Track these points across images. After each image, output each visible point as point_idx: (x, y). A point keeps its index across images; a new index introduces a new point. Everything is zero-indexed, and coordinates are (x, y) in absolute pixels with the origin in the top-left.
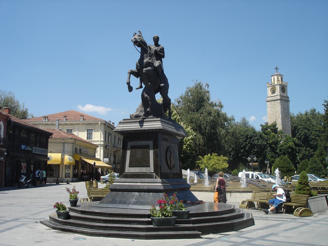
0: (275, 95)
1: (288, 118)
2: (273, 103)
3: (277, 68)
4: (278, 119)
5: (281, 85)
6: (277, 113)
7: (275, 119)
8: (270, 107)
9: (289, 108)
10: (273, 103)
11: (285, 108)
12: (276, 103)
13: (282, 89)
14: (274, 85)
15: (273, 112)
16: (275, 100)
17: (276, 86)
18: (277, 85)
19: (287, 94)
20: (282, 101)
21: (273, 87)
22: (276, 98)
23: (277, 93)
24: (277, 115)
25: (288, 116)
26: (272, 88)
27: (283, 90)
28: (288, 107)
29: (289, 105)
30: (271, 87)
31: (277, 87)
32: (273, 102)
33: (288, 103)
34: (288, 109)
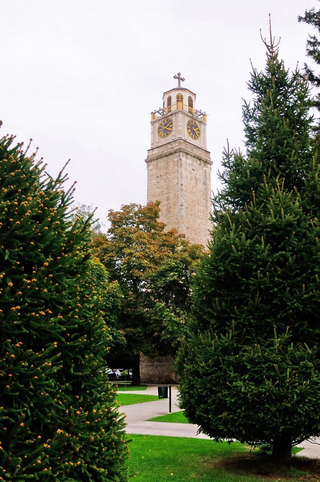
0: (169, 139)
2: (162, 164)
3: (182, 77)
4: (173, 207)
5: (187, 115)
6: (171, 191)
8: (155, 176)
9: (208, 182)
10: (162, 164)
11: (196, 179)
12: (171, 164)
13: (188, 125)
14: (168, 116)
15: (162, 190)
16: (166, 156)
17: (173, 118)
18: (175, 113)
19: (205, 143)
20: (187, 158)
21: (164, 122)
22: (172, 148)
23: (175, 136)
24: (172, 196)
25: (204, 201)
26: (161, 125)
27: (191, 129)
28: (206, 178)
29: (210, 175)
30: (161, 121)
31: (174, 120)
32: (162, 160)
33: (207, 167)
34: (205, 183)
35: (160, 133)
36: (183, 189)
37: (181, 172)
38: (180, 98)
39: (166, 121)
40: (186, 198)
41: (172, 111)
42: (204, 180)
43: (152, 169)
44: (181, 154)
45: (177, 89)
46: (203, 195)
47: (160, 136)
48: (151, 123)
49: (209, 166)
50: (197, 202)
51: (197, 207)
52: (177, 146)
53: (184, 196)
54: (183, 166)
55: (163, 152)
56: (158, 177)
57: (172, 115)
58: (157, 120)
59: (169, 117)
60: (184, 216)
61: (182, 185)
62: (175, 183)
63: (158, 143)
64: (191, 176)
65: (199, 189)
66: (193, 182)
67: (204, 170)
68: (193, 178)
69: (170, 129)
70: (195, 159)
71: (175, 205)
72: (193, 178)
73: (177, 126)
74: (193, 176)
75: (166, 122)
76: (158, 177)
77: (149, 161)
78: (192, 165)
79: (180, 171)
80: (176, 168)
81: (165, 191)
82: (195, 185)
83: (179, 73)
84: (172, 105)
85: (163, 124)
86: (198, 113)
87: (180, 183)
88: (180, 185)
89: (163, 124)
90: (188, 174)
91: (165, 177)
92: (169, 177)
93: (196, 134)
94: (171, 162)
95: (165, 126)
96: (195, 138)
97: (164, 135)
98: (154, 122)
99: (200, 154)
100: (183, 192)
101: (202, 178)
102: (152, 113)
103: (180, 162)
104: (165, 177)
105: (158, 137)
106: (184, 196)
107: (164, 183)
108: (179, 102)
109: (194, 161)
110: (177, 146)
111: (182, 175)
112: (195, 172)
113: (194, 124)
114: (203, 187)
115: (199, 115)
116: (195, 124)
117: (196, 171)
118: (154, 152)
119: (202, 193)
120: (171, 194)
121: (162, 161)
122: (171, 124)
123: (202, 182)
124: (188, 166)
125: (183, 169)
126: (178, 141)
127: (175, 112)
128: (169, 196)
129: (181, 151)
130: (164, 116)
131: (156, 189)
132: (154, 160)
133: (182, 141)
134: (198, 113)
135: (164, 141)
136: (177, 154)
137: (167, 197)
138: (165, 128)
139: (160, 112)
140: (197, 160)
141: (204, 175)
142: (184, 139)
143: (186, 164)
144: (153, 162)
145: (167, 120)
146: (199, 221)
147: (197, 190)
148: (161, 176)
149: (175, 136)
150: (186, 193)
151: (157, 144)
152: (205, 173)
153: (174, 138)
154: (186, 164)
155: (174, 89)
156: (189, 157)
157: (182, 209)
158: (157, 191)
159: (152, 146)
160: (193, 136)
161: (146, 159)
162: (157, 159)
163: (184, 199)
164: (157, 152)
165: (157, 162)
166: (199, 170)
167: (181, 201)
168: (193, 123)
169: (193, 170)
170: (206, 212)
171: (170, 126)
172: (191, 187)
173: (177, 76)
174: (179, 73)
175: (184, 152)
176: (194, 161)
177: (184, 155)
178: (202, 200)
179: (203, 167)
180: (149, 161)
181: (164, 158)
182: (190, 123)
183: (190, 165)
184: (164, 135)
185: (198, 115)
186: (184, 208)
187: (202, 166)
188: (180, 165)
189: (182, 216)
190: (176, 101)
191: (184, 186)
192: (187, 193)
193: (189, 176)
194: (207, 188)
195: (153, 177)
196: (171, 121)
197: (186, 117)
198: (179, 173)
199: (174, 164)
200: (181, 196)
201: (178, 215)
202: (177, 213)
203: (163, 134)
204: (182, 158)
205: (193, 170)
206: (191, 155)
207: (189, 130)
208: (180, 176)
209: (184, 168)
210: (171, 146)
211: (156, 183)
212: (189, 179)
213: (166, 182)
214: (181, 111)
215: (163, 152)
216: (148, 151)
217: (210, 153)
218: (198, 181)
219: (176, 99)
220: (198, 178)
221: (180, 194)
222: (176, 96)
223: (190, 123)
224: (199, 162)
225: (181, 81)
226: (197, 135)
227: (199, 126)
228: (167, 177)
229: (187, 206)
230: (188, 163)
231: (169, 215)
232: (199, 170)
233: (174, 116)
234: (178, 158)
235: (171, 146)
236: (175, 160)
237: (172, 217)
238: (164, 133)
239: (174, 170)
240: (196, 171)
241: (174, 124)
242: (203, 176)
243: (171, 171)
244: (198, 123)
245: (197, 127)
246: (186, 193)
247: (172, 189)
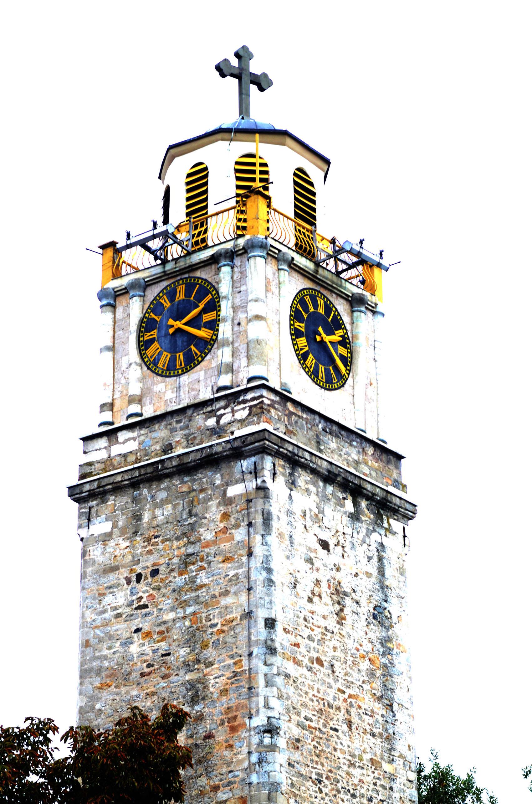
1: (392, 749)
3: (255, 67)
4: (221, 736)
6: (210, 653)
8: (125, 573)
13: (296, 315)
20: (292, 484)
21: (172, 295)
22: (217, 431)
23: (230, 369)
25: (380, 710)
27: (311, 335)
28: (383, 587)
30: (153, 292)
31: (225, 288)
33: (389, 530)
35: (150, 352)
36: (277, 645)
37: (267, 559)
38: (258, 176)
39: (181, 289)
40: (291, 690)
41: (210, 243)
42: (378, 597)
43: (106, 538)
44: (268, 462)
45: (238, 131)
46: (371, 674)
48: (102, 295)
49: (396, 525)
50: (342, 715)
51: (345, 740)
52: (243, 422)
53: (279, 680)
54: (275, 524)
55: (168, 448)
56: (139, 577)
57: (214, 260)
58: (134, 285)
59: (198, 274)
60: (284, 788)
61: (270, 623)
62: (236, 614)
63: (139, 400)
64: (315, 575)
65: (351, 645)
67: (374, 546)
68: (324, 585)
69: (203, 333)
70: (330, 489)
71: (233, 729)
72: (324, 585)
73: (242, 316)
74: (324, 575)
75: (181, 295)
76: (139, 577)
77: (92, 495)
78: (317, 519)
79: (259, 550)
80: (240, 534)
81: (183, 652)
82: (332, 623)
83: (244, 48)
84: (211, 210)
85: (167, 304)
86: (343, 256)
87: (261, 614)
88: (261, 623)
89: (167, 304)
91: (179, 581)
92: (203, 578)
93: (333, 361)
94: (213, 504)
95: (178, 318)
96: (329, 380)
97: (173, 360)
98: (124, 292)
99: (357, 463)
100: (277, 660)
102: (103, 247)
103: (259, 504)
104: (179, 581)
106: (279, 680)
107: (173, 609)
108: (253, 197)
109: (325, 498)
110: (243, 422)
111: (269, 571)
113: (321, 311)
114: (371, 635)
115: (350, 267)
116: (329, 308)
117: (339, 549)
118: (116, 450)
119: (365, 665)
120: (214, 670)
121: (162, 495)
122: (214, 306)
123: (366, 608)
124: (299, 525)
125: (272, 539)
126: (249, 396)
127: (229, 246)
128: (203, 681)
129: (263, 451)
130: (169, 267)
131: (128, 642)
132: (117, 489)
133: (268, 397)
134: (343, 256)
135: (170, 395)
136: (246, 464)
137: (191, 686)
138: (179, 324)
139: (155, 244)
140: (340, 495)
141: (375, 572)
142: (278, 388)
143: (289, 513)
144: (111, 500)
145: (189, 289)
147: (345, 651)
148: (155, 573)
149: (230, 369)
150: (290, 668)
151: (135, 408)
152: (380, 559)
153: (225, 380)
154: (289, 513)
155: (220, 131)
156: (303, 478)
157: (273, 748)
158: (134, 649)
159: (107, 416)
160: (322, 368)
161: (75, 481)
162: (135, 484)
163: (280, 697)
164: (132, 446)
165: (135, 500)
166: (353, 547)
167: (267, 706)
168: (321, 302)
169: (325, 545)
170: (387, 767)
171: (207, 317)
172: (317, 634)
173: (235, 62)
174: (244, 48)
175: (277, 454)
176: (325, 498)
177: (279, 470)
178: (368, 703)
179: (368, 534)
180: (92, 495)
181: (176, 482)
182: (302, 302)
183: (309, 523)
184: (173, 360)
185: (342, 267)
186: (281, 742)
187: (363, 528)
188: (259, 520)
189: (274, 787)
190: (233, 191)
191: (279, 627)
192: (297, 662)
194: (388, 640)
195: (112, 578)
196: (207, 293)
197: (285, 276)
198: (256, 563)
199: (226, 516)
200: (269, 683)
201: (254, 778)
202: (249, 770)
203: (166, 357)
204: (269, 484)
205: (325, 545)
206: (314, 471)
207: (302, 342)
208: (258, 577)
209: (281, 535)
210: (211, 422)
211: (128, 610)
213: (184, 604)
214: (263, 246)
215: (168, 448)
216: (86, 439)
217: (399, 457)
218: (348, 601)
219: (233, 182)
220: (346, 587)
221: (263, 669)
222: (232, 167)
223: (302, 302)
224: (349, 506)
225: (253, 88)
226: (336, 369)
227: (346, 319)
228: (193, 580)
229: (296, 732)
230: (299, 513)
231: (203, 781)
232: (353, 547)
233: (225, 271)
234: (252, 485)
235: (211, 422)
236: (234, 491)
237: (216, 789)
238: (173, 350)
239: (225, 546)
240: (339, 549)
241: (225, 308)
242: (369, 575)
243: (212, 550)
244: (341, 307)
245: (338, 324)
246: (290, 668)
247: (216, 644)
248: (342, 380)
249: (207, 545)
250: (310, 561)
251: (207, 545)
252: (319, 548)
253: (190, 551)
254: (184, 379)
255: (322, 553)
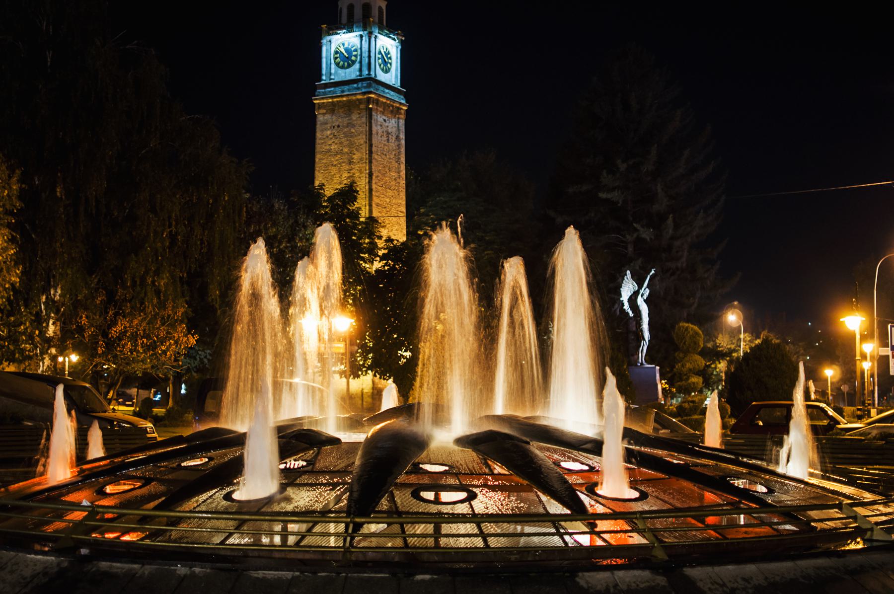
7: (346, 175)
8: (328, 126)
11: (388, 133)
25: (397, 165)
47: (337, 64)
66: (385, 138)
74: (385, 129)
90: (379, 127)
97: (344, 64)
101: (394, 130)
105: (333, 66)
112: (387, 124)
119: (394, 153)
141: (396, 126)
146: (390, 193)
148: (339, 126)
169: (385, 120)
184: (344, 64)
193: (380, 131)
195: (326, 126)
205: (385, 120)
212: (380, 136)
218: (390, 136)
248: (389, 69)
249: (354, 121)
250: (381, 126)
251: (354, 121)
252: (383, 121)
253: (349, 121)
254: (347, 70)
255: (384, 123)
